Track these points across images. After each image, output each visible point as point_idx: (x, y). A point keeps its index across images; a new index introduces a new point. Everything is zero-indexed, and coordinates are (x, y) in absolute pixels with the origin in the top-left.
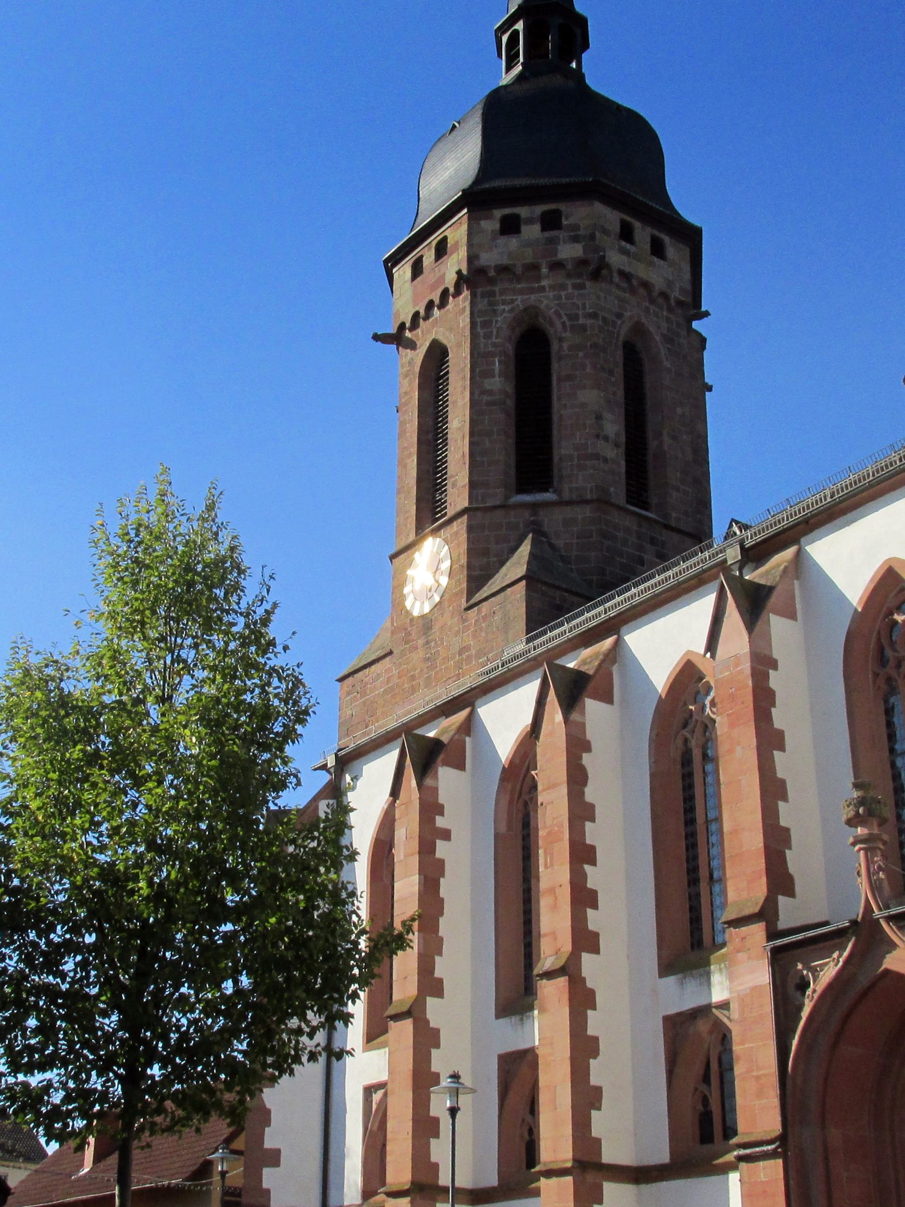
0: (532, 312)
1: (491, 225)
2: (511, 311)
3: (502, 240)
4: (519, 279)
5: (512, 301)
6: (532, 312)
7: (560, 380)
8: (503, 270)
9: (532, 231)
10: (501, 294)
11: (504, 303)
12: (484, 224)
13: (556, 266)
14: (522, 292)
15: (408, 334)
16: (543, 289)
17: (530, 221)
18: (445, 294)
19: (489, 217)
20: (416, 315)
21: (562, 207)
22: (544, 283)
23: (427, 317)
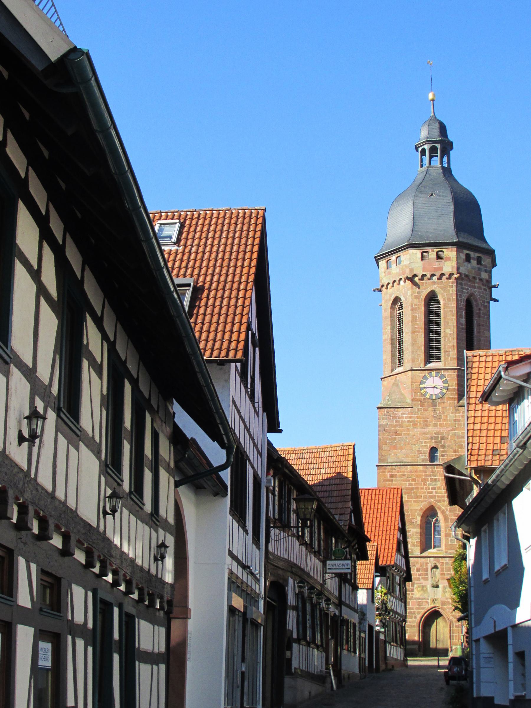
0: (472, 295)
1: (463, 256)
2: (467, 293)
3: (466, 264)
4: (470, 281)
5: (467, 289)
6: (472, 295)
7: (479, 325)
8: (466, 276)
9: (474, 263)
10: (465, 285)
11: (465, 289)
12: (461, 255)
13: (481, 280)
14: (469, 286)
15: (416, 279)
16: (475, 287)
17: (474, 259)
18: (442, 275)
19: (462, 253)
20: (424, 275)
21: (482, 256)
22: (476, 285)
23: (429, 279)
